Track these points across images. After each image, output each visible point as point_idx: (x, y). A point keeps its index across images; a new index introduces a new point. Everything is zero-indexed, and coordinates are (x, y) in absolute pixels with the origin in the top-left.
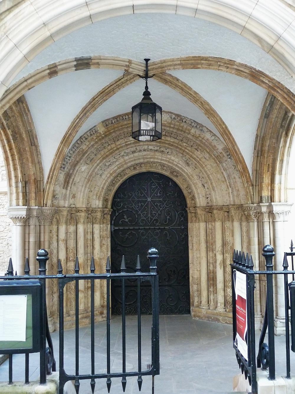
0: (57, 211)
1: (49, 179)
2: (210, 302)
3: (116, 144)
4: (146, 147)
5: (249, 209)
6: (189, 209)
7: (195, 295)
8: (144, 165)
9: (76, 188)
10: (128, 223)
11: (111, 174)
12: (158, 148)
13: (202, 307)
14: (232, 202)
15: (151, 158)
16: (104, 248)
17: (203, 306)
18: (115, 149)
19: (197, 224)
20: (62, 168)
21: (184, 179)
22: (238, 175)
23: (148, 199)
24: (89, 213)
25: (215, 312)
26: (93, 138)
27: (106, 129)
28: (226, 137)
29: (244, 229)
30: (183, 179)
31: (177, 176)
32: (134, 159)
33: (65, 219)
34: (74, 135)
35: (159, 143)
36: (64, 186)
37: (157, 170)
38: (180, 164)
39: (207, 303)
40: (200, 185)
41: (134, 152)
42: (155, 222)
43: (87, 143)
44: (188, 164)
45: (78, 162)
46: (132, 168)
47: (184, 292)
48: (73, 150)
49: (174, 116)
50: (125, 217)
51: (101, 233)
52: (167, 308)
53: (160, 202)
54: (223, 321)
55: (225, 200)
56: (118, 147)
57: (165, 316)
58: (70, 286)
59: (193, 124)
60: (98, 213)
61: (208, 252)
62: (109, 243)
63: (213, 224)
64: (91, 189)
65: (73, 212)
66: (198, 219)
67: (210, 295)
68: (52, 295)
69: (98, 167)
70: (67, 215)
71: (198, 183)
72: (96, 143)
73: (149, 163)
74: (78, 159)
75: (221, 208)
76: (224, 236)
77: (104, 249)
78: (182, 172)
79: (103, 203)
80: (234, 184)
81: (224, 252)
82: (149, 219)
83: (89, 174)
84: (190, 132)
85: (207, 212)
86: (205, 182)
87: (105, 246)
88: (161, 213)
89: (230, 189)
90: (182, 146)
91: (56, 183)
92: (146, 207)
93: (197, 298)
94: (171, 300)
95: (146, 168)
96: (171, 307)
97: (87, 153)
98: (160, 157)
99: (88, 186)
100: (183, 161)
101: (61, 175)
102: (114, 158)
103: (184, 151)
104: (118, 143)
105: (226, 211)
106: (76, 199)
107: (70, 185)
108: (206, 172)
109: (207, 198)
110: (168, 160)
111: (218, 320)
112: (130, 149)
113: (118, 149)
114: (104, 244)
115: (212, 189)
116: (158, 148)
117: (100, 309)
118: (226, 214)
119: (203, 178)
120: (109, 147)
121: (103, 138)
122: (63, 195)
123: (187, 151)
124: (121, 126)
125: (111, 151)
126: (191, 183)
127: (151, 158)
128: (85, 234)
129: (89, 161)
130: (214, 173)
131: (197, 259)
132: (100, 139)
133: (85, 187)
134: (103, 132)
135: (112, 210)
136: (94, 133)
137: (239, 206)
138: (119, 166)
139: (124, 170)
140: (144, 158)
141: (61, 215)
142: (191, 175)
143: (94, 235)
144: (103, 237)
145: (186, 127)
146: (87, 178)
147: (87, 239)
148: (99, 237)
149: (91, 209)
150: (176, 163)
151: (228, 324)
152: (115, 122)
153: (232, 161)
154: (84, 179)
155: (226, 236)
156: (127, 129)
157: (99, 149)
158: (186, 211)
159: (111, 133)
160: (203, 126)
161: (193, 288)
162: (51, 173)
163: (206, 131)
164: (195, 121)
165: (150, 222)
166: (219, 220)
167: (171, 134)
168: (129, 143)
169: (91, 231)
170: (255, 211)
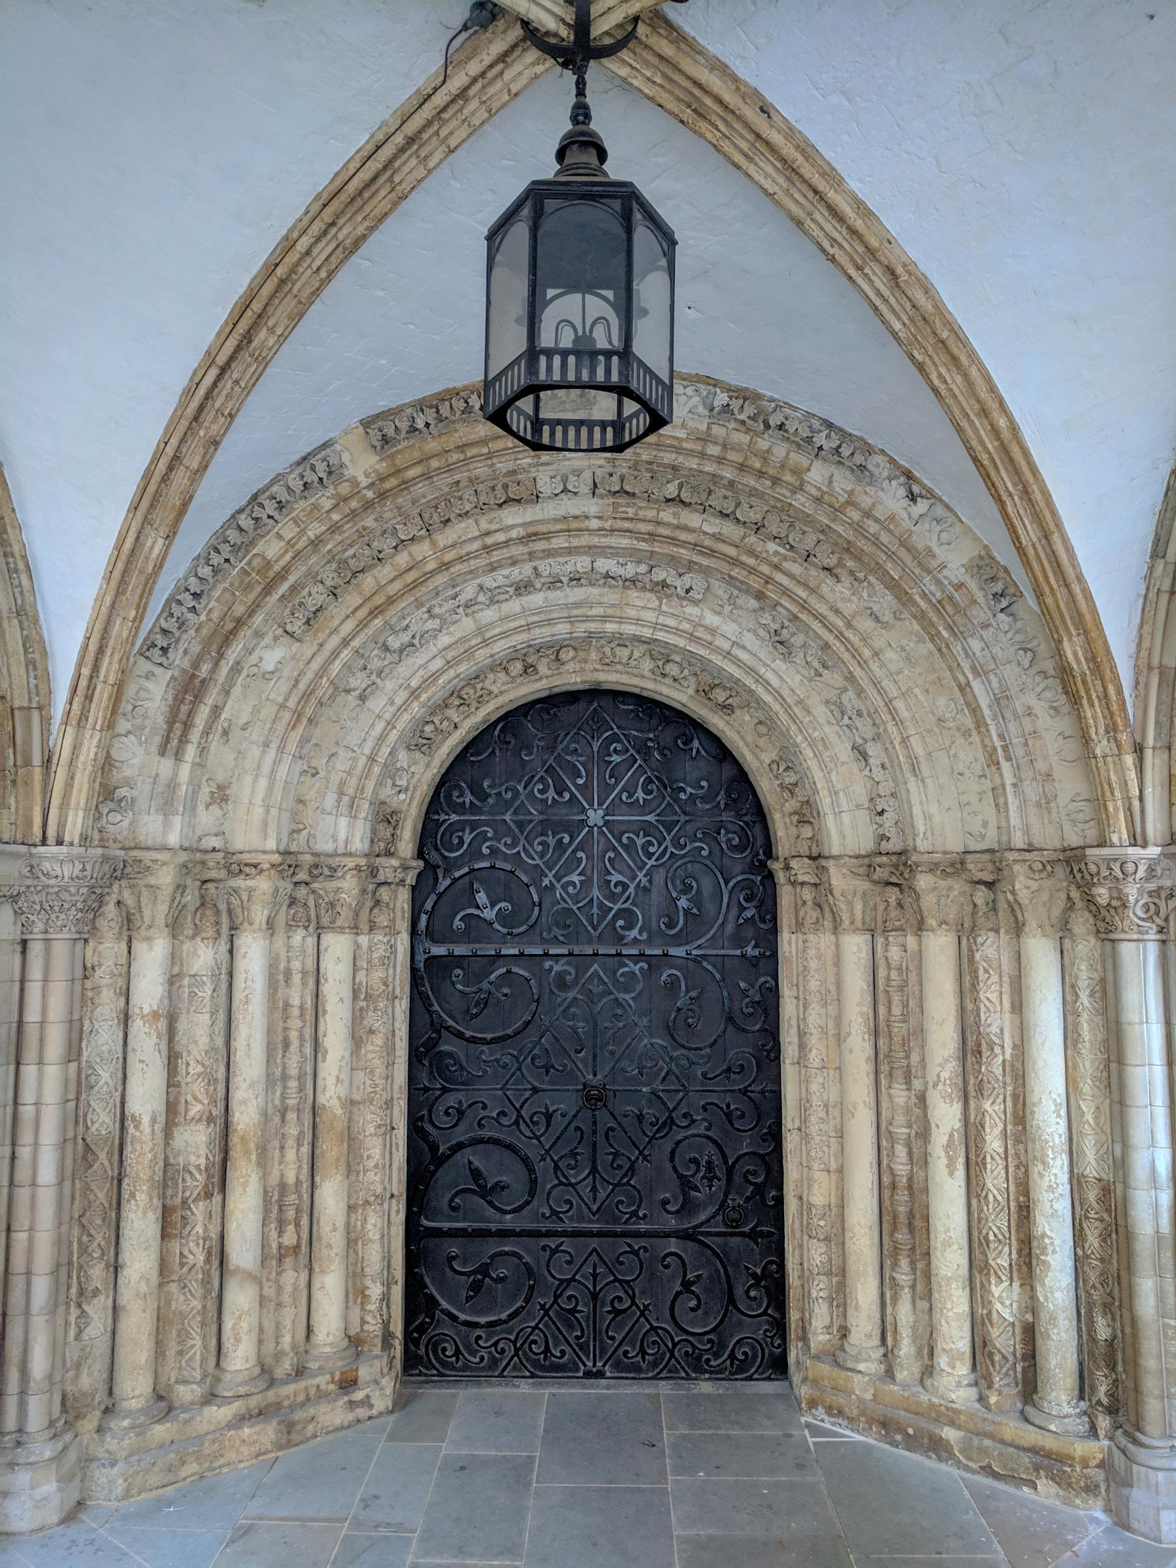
0: (119, 869)
1: (76, 699)
3: (434, 544)
4: (582, 563)
5: (1121, 876)
6: (787, 868)
7: (814, 1294)
8: (571, 654)
9: (233, 756)
10: (497, 926)
11: (414, 694)
12: (643, 568)
13: (850, 1364)
14: (1019, 834)
15: (604, 618)
17: (857, 1359)
18: (431, 566)
19: (823, 941)
20: (156, 652)
21: (760, 722)
22: (1048, 694)
23: (591, 813)
26: (315, 507)
28: (1009, 485)
29: (1084, 975)
31: (726, 708)
32: (523, 622)
35: (644, 540)
36: (167, 740)
37: (636, 681)
39: (876, 1341)
40: (843, 751)
41: (523, 588)
42: (621, 923)
43: (289, 531)
46: (517, 668)
47: (759, 1271)
49: (722, 398)
50: (482, 898)
53: (646, 829)
54: (969, 1459)
55: (975, 825)
56: (449, 556)
57: (664, 1388)
59: (820, 439)
60: (343, 877)
62: (397, 1025)
65: (213, 874)
66: (828, 915)
68: (79, 1305)
69: (346, 654)
70: (180, 888)
71: (833, 738)
72: (335, 528)
74: (239, 610)
78: (753, 687)
79: (374, 831)
80: (1026, 744)
81: (971, 1088)
82: (595, 910)
83: (302, 686)
84: (802, 482)
85: (875, 883)
86: (869, 736)
88: (650, 881)
89: (1005, 766)
90: (757, 557)
91: (123, 725)
92: (580, 854)
94: (692, 1310)
95: (583, 670)
98: (650, 616)
99: (292, 747)
101: (149, 685)
104: (444, 538)
105: (986, 877)
106: (230, 807)
108: (876, 684)
109: (881, 813)
110: (686, 626)
111: (938, 1447)
112: (506, 572)
113: (445, 566)
114: (371, 1032)
115: (906, 768)
116: (643, 568)
117: (339, 1364)
118: (981, 896)
120: (402, 559)
122: (160, 788)
125: (410, 578)
126: (799, 739)
127: (604, 618)
128: (277, 982)
129: (300, 623)
130: (916, 690)
131: (822, 1114)
132: (353, 511)
133: (281, 749)
136: (321, 479)
137: (1055, 856)
138: (451, 654)
140: (571, 620)
142: (800, 702)
143: (321, 988)
144: (368, 996)
145: (784, 454)
146: (291, 704)
148: (347, 993)
150: (726, 646)
151: (996, 1476)
153: (1019, 624)
155: (983, 1009)
157: (351, 562)
158: (770, 876)
159: (405, 485)
160: (869, 450)
161: (804, 1255)
162: (86, 672)
163: (886, 473)
164: (830, 425)
165: (599, 923)
167: (704, 496)
168: (500, 537)
169: (310, 965)
170: (1152, 886)
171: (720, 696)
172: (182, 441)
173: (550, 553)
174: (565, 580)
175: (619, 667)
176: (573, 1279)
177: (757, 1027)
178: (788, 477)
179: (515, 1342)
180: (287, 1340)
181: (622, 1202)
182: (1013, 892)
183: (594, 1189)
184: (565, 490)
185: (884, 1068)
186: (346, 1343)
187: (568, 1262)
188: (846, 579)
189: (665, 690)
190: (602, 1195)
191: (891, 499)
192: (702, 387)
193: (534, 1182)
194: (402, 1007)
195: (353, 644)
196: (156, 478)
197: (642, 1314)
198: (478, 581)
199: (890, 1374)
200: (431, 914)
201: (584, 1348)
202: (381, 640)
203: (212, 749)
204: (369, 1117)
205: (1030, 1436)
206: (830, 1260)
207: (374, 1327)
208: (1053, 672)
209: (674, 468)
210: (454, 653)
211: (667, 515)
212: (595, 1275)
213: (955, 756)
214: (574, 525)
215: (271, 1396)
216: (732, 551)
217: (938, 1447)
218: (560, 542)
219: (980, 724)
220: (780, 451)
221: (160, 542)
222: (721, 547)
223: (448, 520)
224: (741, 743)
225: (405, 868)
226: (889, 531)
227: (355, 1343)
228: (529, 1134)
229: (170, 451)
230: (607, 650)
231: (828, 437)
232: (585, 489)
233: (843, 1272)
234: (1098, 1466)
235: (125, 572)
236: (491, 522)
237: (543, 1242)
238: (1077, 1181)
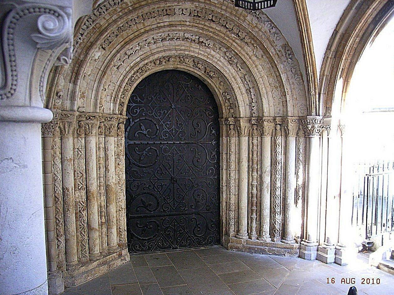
3: (144, 25)
6: (227, 120)
15: (185, 50)
18: (142, 31)
30: (220, 81)
37: (188, 68)
44: (230, 62)
50: (143, 127)
51: (116, 148)
56: (147, 28)
67: (251, 223)
68: (57, 239)
73: (179, 58)
74: (92, 40)
77: (119, 171)
87: (121, 167)
90: (229, 38)
94: (198, 231)
97: (106, 31)
98: (197, 51)
100: (226, 58)
102: (138, 44)
113: (147, 32)
116: (197, 37)
123: (236, 45)
125: (136, 34)
127: (185, 50)
133: (100, 82)
138: (142, 57)
151: (276, 254)
154: (98, 70)
156: (166, 3)
163: (266, 20)
168: (162, 24)
176: (169, 226)
178: (242, 18)
181: (181, 207)
189: (196, 71)
193: (158, 203)
199: (250, 238)
214: (183, 23)
216: (223, 35)
217: (263, 252)
228: (157, 191)
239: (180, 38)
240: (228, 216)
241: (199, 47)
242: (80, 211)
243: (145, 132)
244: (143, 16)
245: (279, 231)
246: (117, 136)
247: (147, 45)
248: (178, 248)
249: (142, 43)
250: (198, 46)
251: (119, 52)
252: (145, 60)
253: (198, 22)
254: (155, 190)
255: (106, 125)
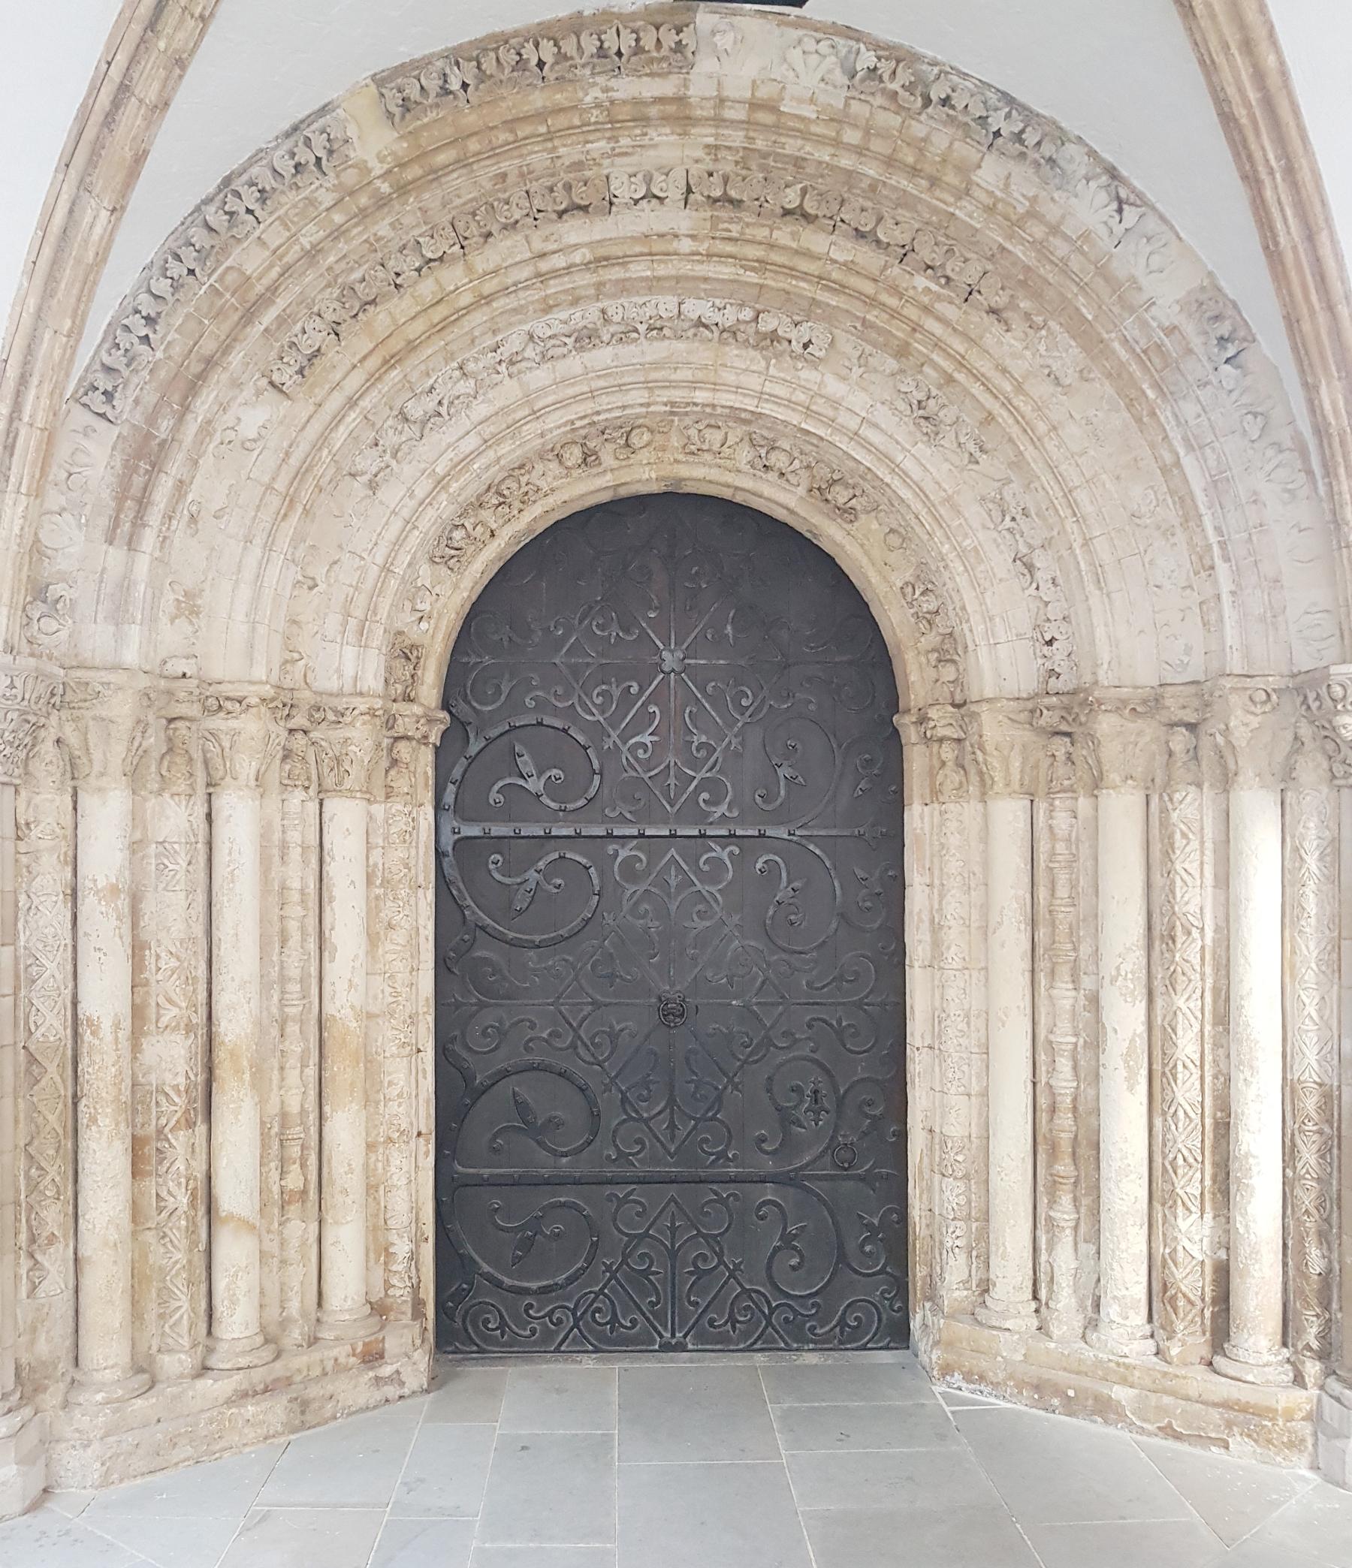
2: (1051, 1291)
3: (469, 269)
4: (666, 305)
6: (923, 720)
8: (646, 437)
10: (545, 800)
15: (694, 385)
16: (389, 946)
17: (1004, 1315)
18: (466, 299)
19: (971, 809)
21: (892, 531)
24: (291, 725)
25: (1089, 1354)
27: (402, 137)
28: (1271, 156)
31: (847, 513)
32: (586, 389)
33: (119, 750)
34: (152, 96)
35: (753, 269)
36: (116, 522)
37: (729, 478)
38: (883, 426)
40: (1000, 562)
41: (585, 339)
42: (705, 796)
45: (210, 363)
46: (574, 455)
48: (176, 270)
52: (772, 1310)
54: (1144, 1420)
56: (488, 287)
58: (164, 1194)
59: (997, 121)
60: (352, 724)
61: (1043, 980)
62: (421, 922)
63: (1084, 804)
64: (310, 573)
66: (974, 778)
74: (208, 346)
75: (1151, 703)
76: (1158, 880)
77: (390, 957)
78: (887, 480)
79: (389, 669)
82: (672, 781)
85: (1041, 731)
86: (1037, 542)
87: (400, 937)
88: (742, 743)
89: (1222, 569)
90: (901, 296)
91: (55, 499)
92: (652, 708)
93: (962, 1258)
94: (794, 1268)
96: (789, 1306)
98: (754, 382)
99: (283, 542)
100: (902, 406)
101: (88, 444)
103: (914, 330)
104: (485, 259)
107: (154, 517)
109: (1050, 643)
111: (1104, 1409)
113: (488, 299)
114: (390, 926)
116: (747, 314)
117: (362, 1333)
118: (1180, 740)
119: (1025, 513)
120: (427, 288)
121: (382, 203)
124: (510, 124)
125: (438, 314)
127: (694, 385)
129: (291, 371)
131: (963, 1026)
132: (362, 210)
133: (268, 547)
134: (381, 160)
135: (444, 715)
137: (1281, 683)
138: (489, 430)
139: (520, 467)
140: (649, 386)
141: (94, 718)
144: (385, 883)
146: (280, 485)
147: (284, 887)
149: (307, 694)
150: (853, 424)
152: (465, 86)
156: (549, 145)
159: (435, 175)
165: (678, 796)
166: (1130, 782)
168: (559, 261)
171: (840, 495)
172: (133, 61)
173: (624, 287)
174: (642, 328)
175: (708, 457)
176: (646, 1234)
177: (876, 925)
179: (574, 1312)
180: (294, 1307)
181: (706, 1140)
182: (1227, 731)
183: (672, 1126)
184: (650, 196)
185: (1043, 965)
186: (367, 1309)
187: (638, 1214)
188: (1018, 325)
189: (767, 491)
190: (682, 1132)
191: (1087, 208)
192: (840, 41)
193: (595, 1117)
194: (427, 899)
195: (361, 403)
196: (97, 117)
197: (732, 1276)
198: (526, 327)
200: (460, 784)
201: (660, 1316)
202: (398, 405)
203: (176, 541)
204: (389, 1034)
205: (1221, 1388)
206: (969, 1202)
207: (401, 1292)
208: (1289, 444)
209: (798, 162)
210: (493, 429)
211: (783, 235)
212: (673, 1229)
213: (1151, 563)
214: (658, 246)
215: (279, 1369)
216: (868, 288)
217: (1104, 1409)
218: (639, 270)
219: (1190, 516)
220: (941, 140)
221: (104, 214)
222: (853, 281)
223: (489, 234)
224: (865, 561)
225: (430, 721)
226: (1083, 253)
227: (379, 1310)
229: (115, 74)
230: (693, 432)
231: (1008, 116)
232: (676, 194)
233: (986, 1217)
234: (1303, 1419)
235: (56, 263)
236: (546, 239)
237: (608, 1190)
238: (1290, 1090)
239: (661, 329)
240: (933, 1199)
241: (763, 363)
242: (160, 1131)
243: (535, 785)
244: (457, 223)
245: (1198, 1302)
246: (388, 797)
247: (503, 368)
248: (690, 1347)
249: (476, 360)
250: (759, 357)
251: (356, 403)
252: (498, 443)
253: (735, 230)
254: (578, 1055)
255: (323, 743)
